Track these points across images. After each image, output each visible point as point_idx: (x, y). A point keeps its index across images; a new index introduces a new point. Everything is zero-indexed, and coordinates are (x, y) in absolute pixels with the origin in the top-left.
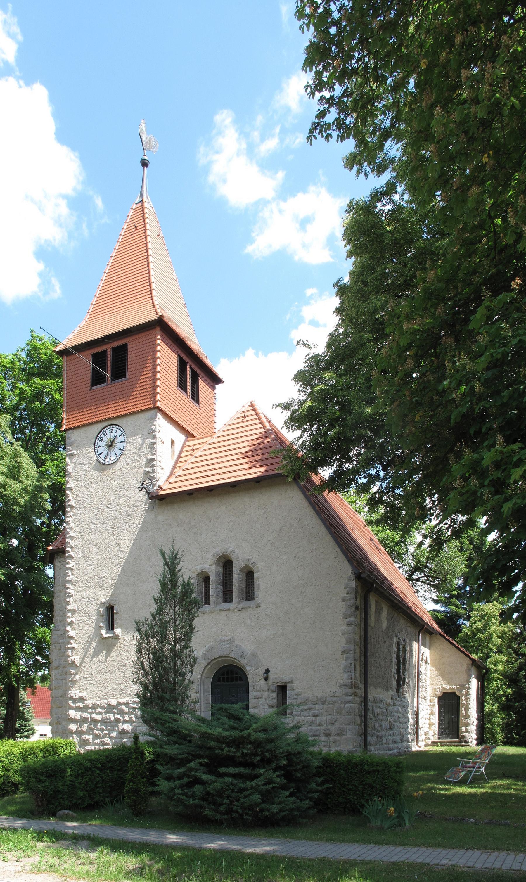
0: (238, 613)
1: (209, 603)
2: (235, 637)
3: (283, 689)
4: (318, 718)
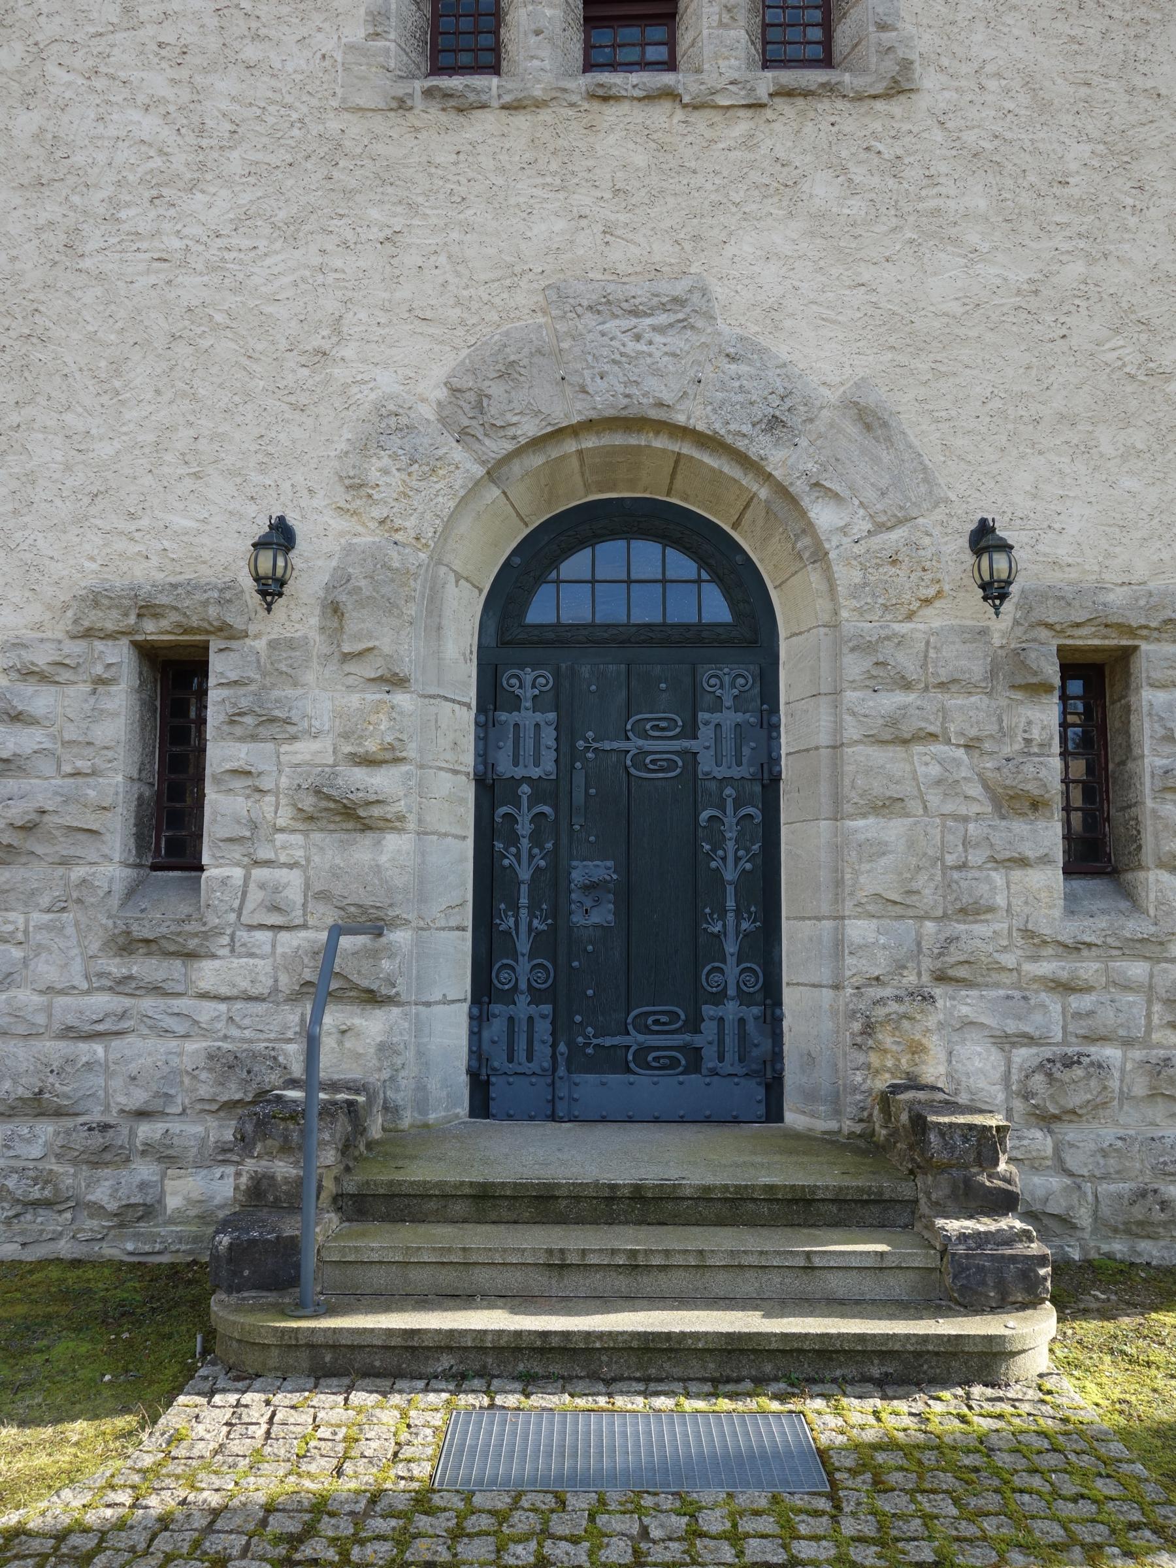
0: (742, 125)
1: (490, 61)
2: (719, 291)
3: (1094, 683)
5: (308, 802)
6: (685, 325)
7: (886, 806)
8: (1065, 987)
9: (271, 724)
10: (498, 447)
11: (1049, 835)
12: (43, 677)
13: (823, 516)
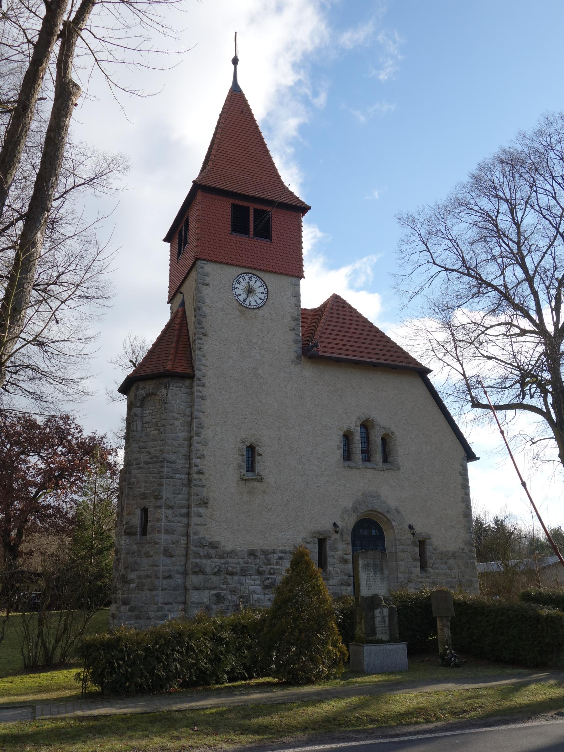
0: (382, 473)
3: (422, 544)
4: (453, 571)
5: (341, 560)
6: (378, 499)
7: (402, 560)
8: (421, 582)
9: (335, 549)
10: (359, 514)
11: (418, 564)
12: (308, 543)
13: (394, 523)
